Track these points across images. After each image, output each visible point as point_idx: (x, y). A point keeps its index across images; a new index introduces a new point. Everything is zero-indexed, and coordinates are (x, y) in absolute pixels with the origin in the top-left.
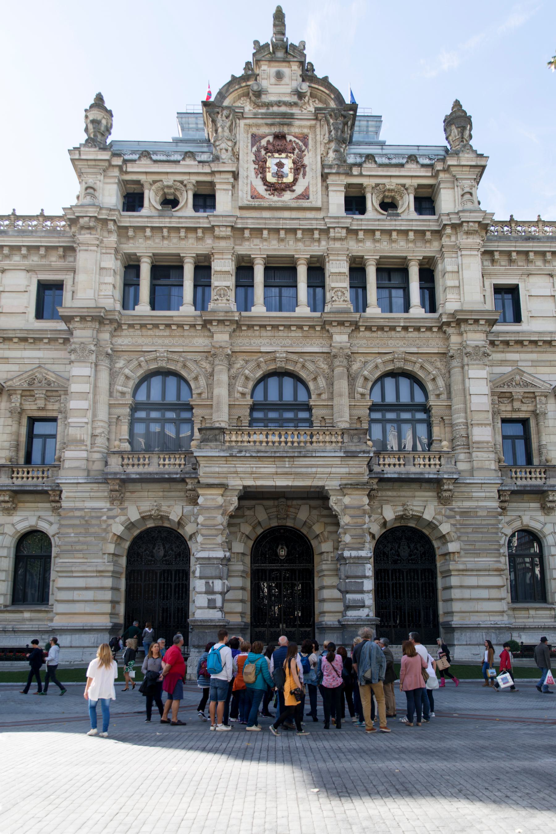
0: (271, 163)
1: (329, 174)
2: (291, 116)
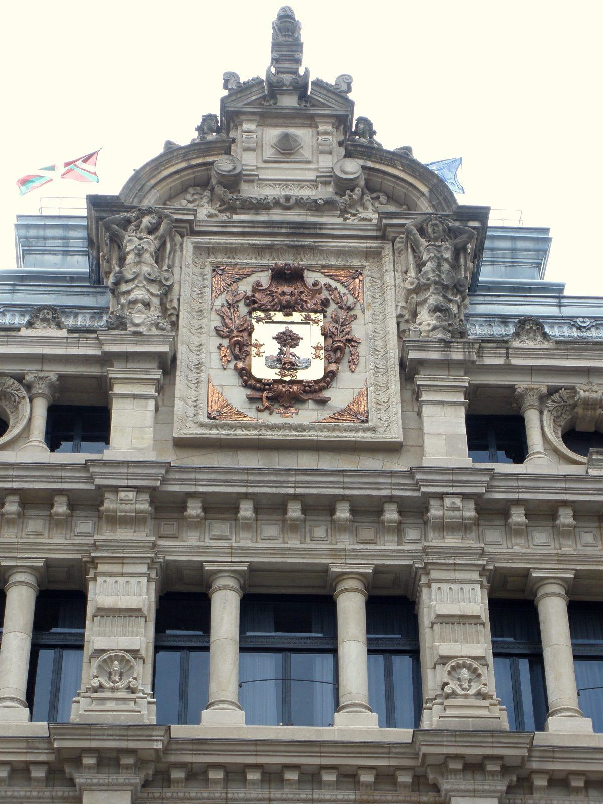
1: (421, 363)
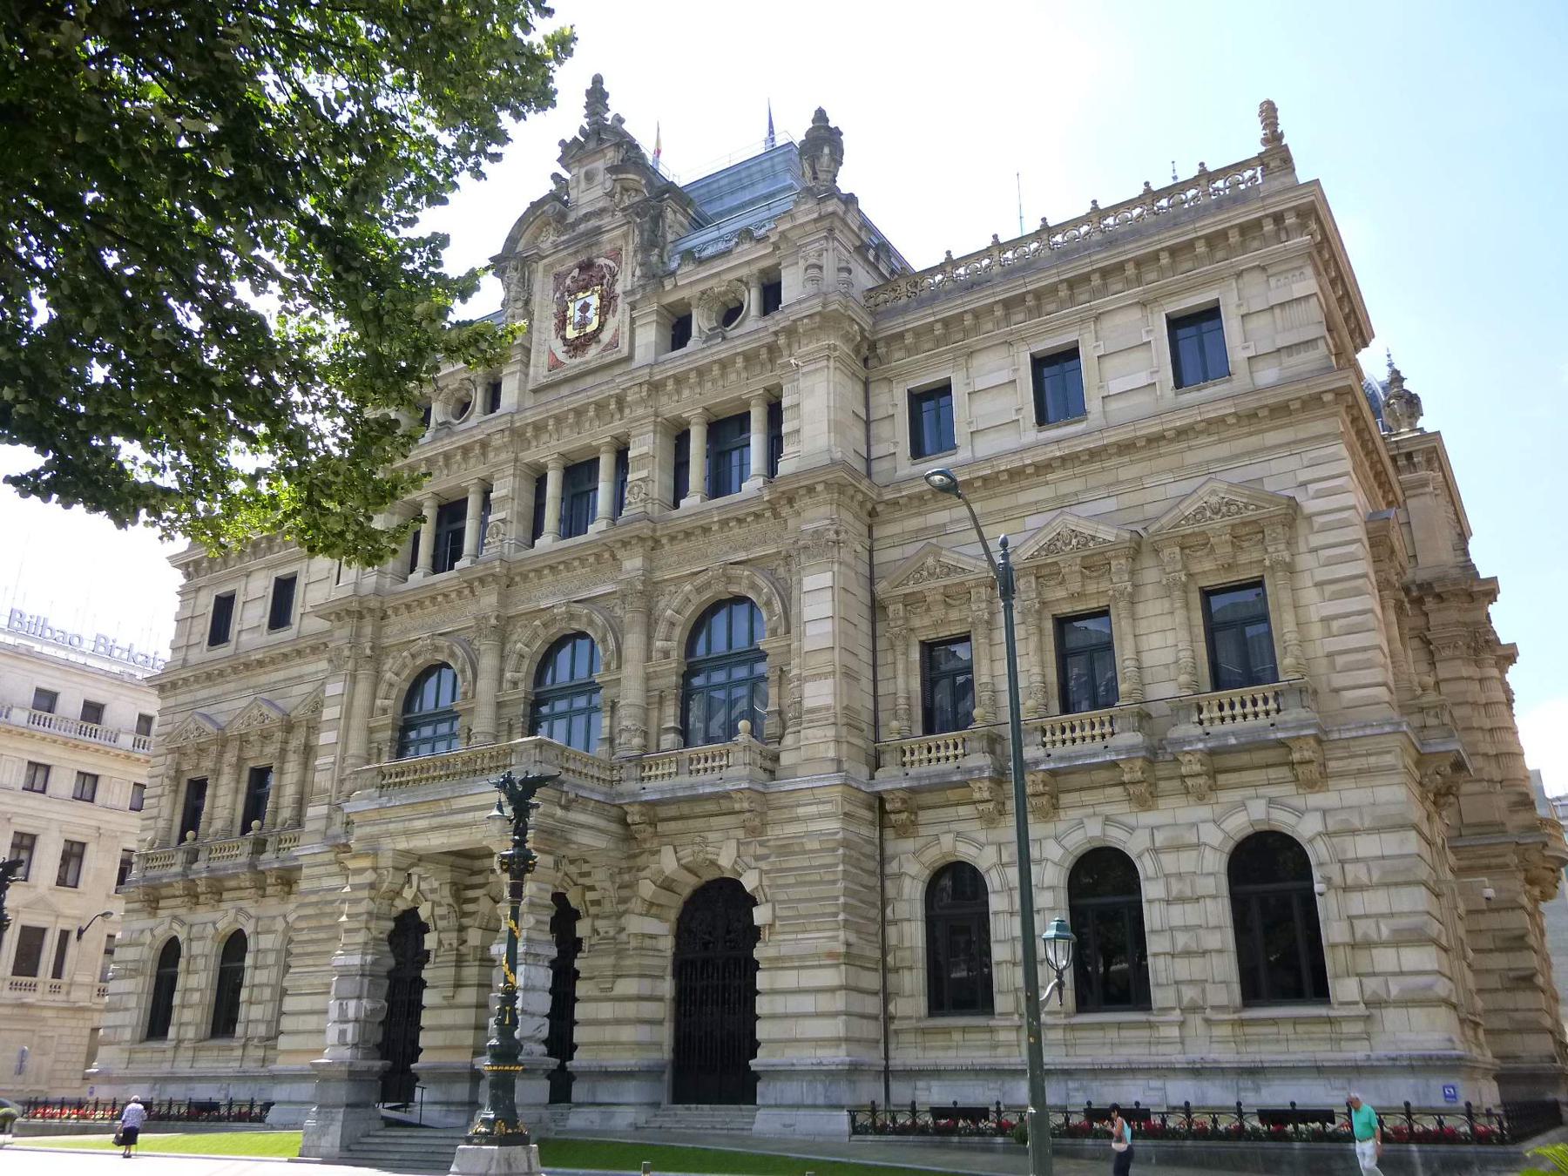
0: (573, 311)
2: (598, 231)
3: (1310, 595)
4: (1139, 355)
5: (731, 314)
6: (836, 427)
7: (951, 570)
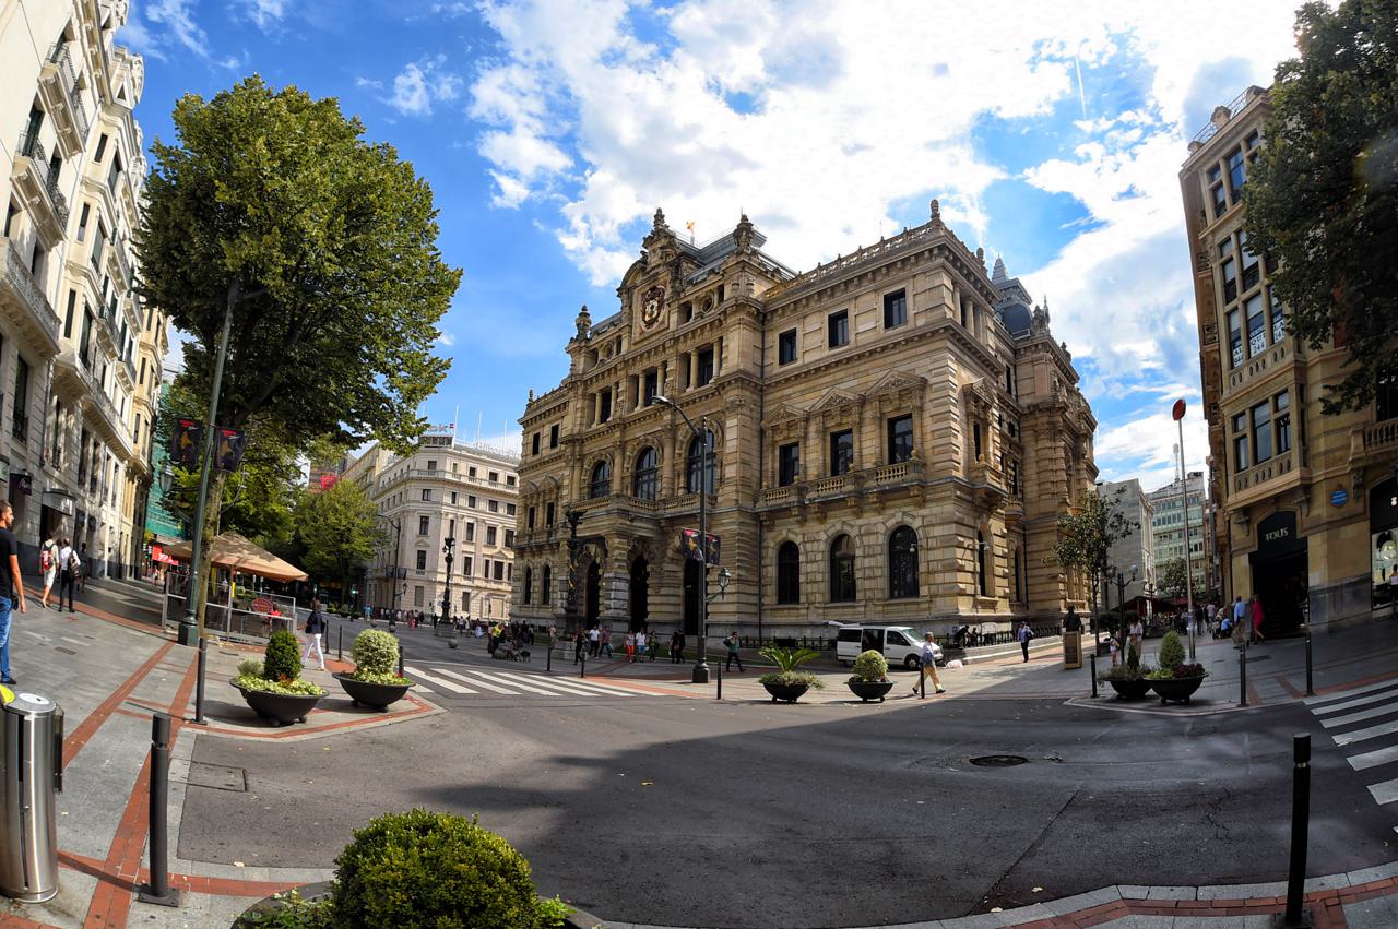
0: (648, 310)
2: (657, 274)
3: (928, 421)
4: (872, 314)
5: (708, 305)
6: (742, 354)
7: (790, 415)
